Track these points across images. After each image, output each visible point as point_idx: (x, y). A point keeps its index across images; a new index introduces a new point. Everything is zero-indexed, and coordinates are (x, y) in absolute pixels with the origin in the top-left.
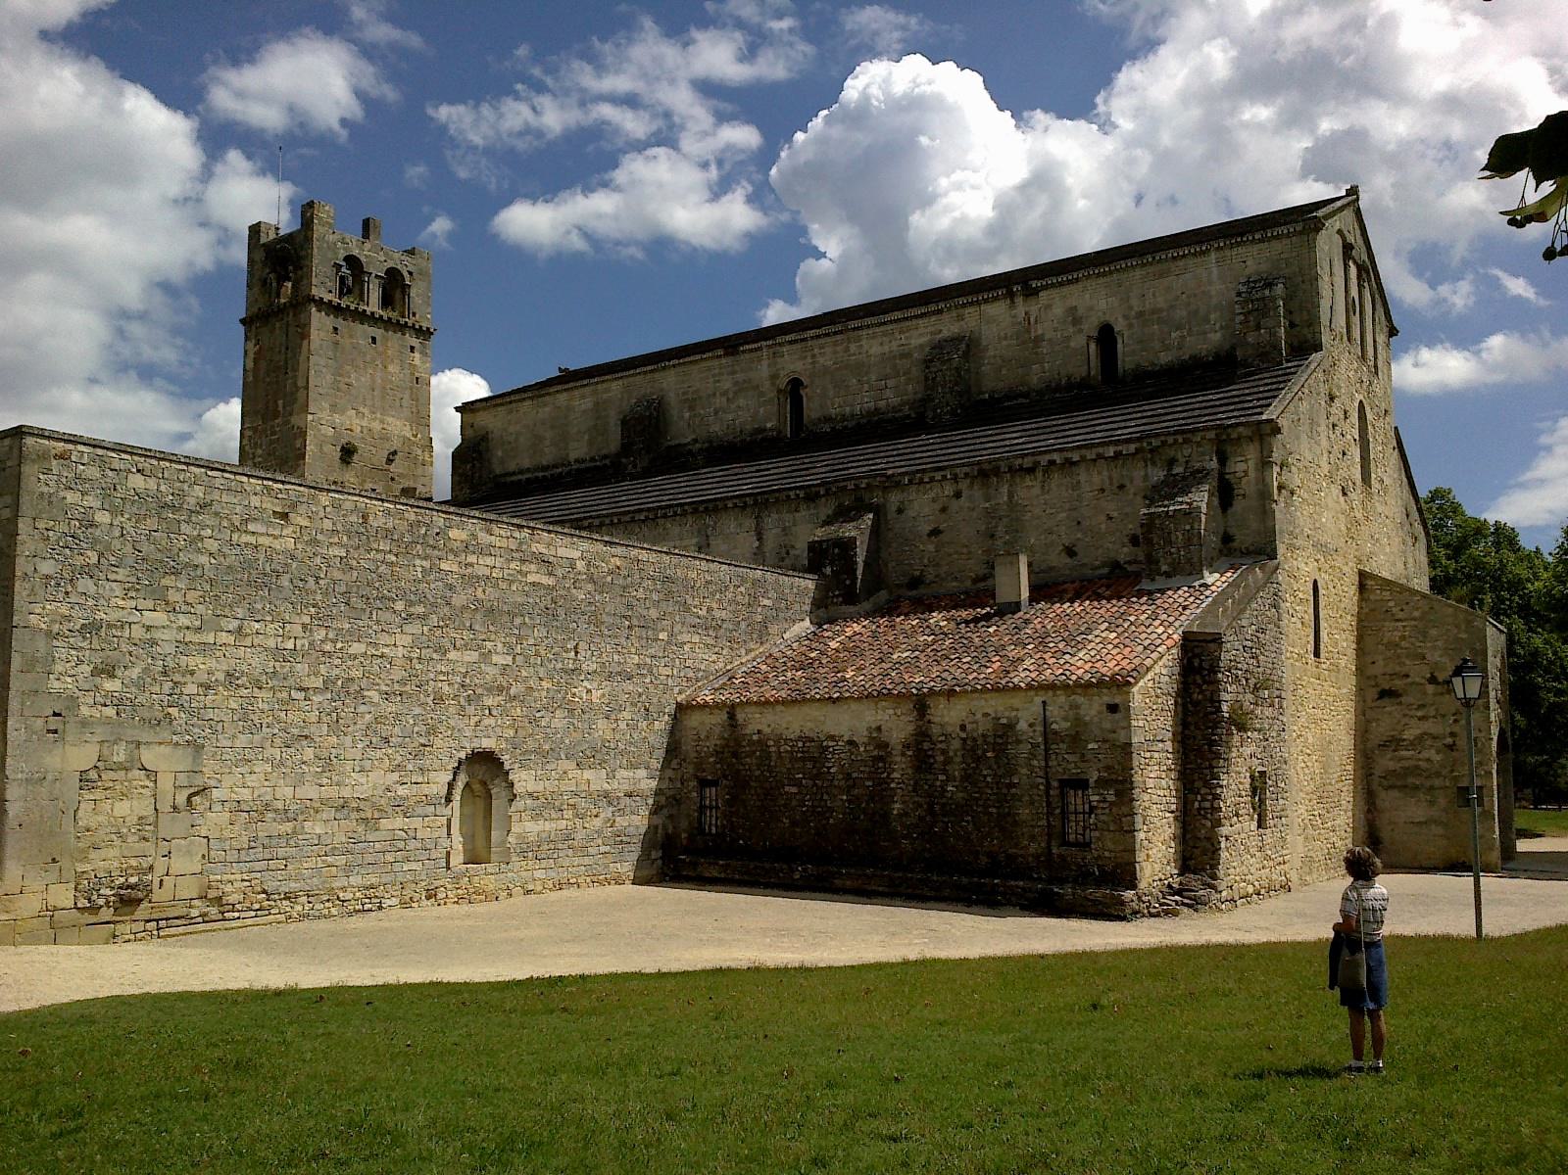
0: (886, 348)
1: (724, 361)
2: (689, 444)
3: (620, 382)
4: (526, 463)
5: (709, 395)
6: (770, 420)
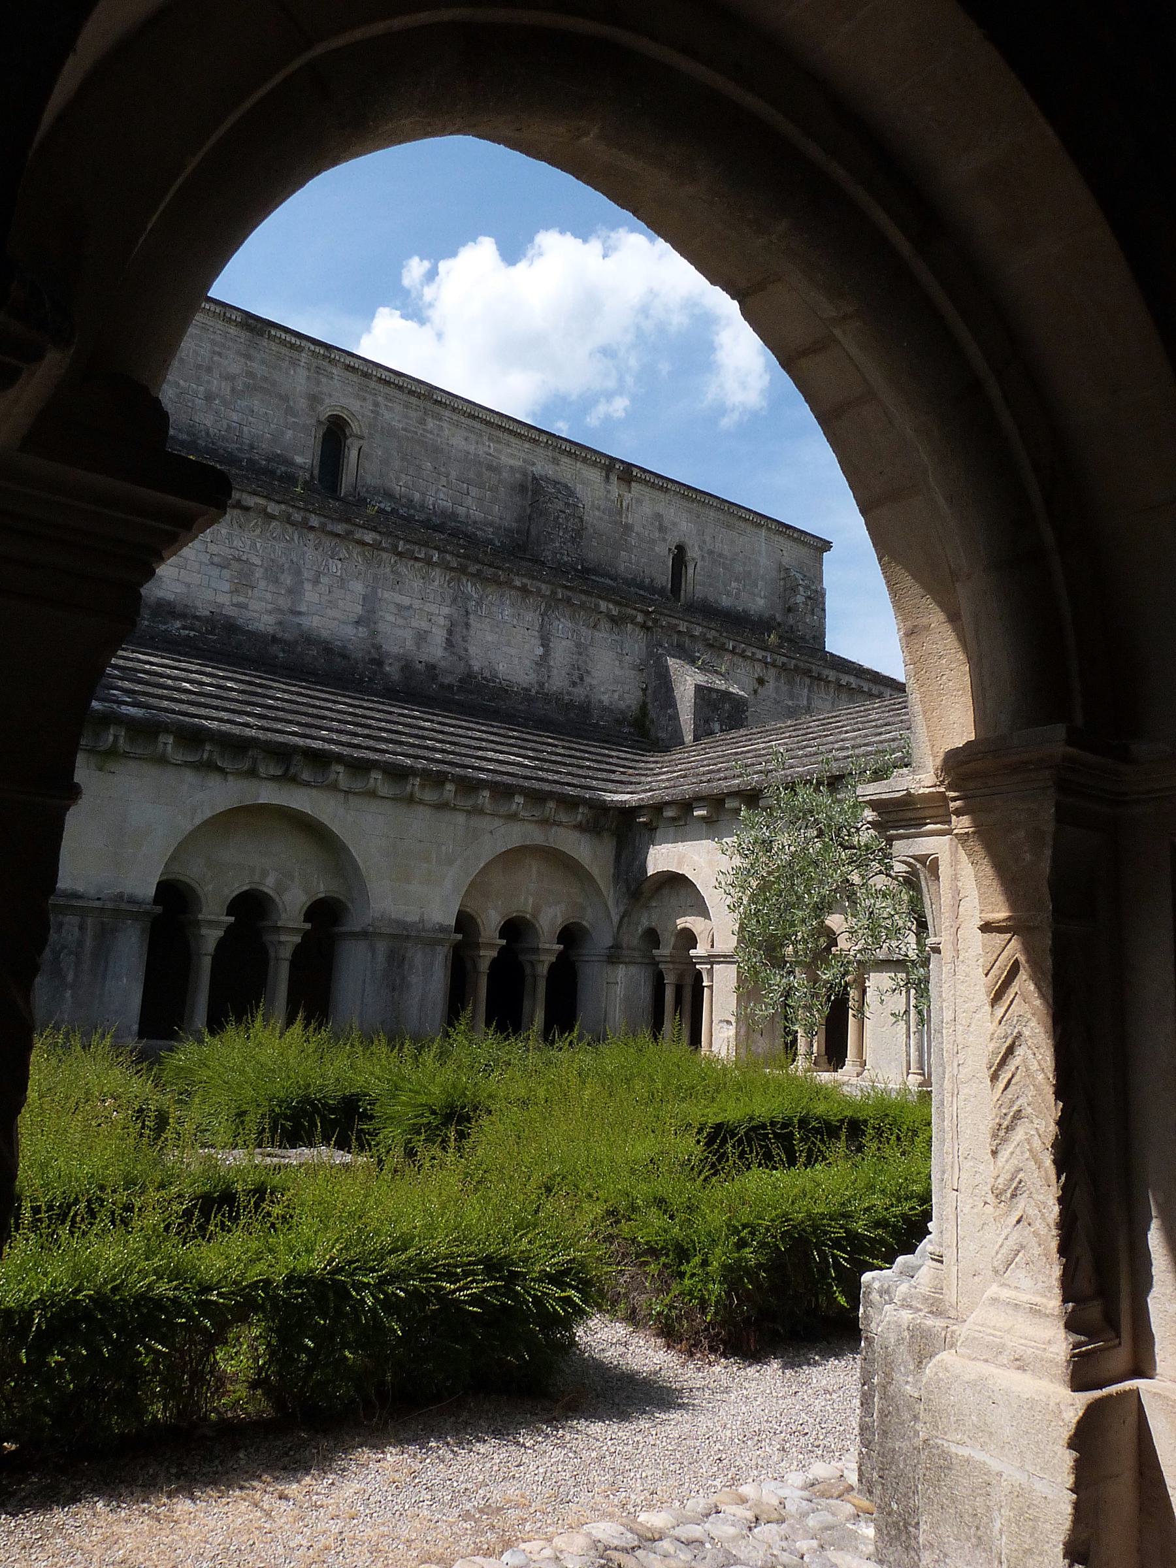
0: (472, 448)
1: (233, 331)
5: (199, 367)
6: (302, 454)
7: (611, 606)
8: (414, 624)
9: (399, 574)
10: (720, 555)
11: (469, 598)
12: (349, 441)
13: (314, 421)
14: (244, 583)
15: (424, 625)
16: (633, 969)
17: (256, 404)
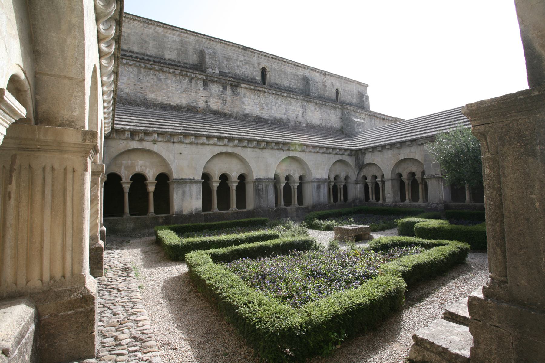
0: (292, 71)
1: (241, 50)
2: (226, 73)
3: (195, 37)
4: (136, 49)
5: (235, 60)
6: (258, 77)
7: (334, 105)
8: (296, 113)
9: (291, 102)
10: (346, 90)
11: (305, 106)
12: (266, 73)
13: (259, 69)
14: (262, 108)
15: (297, 113)
16: (360, 185)
17: (247, 66)
